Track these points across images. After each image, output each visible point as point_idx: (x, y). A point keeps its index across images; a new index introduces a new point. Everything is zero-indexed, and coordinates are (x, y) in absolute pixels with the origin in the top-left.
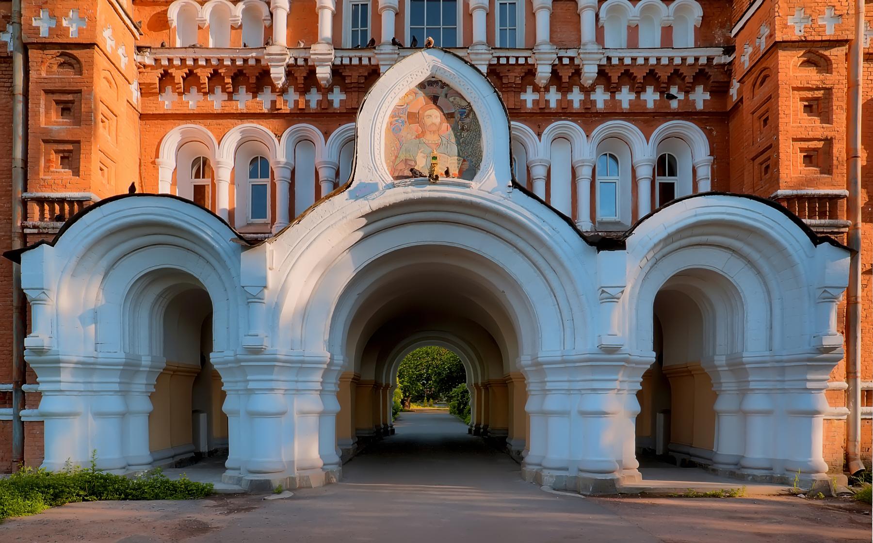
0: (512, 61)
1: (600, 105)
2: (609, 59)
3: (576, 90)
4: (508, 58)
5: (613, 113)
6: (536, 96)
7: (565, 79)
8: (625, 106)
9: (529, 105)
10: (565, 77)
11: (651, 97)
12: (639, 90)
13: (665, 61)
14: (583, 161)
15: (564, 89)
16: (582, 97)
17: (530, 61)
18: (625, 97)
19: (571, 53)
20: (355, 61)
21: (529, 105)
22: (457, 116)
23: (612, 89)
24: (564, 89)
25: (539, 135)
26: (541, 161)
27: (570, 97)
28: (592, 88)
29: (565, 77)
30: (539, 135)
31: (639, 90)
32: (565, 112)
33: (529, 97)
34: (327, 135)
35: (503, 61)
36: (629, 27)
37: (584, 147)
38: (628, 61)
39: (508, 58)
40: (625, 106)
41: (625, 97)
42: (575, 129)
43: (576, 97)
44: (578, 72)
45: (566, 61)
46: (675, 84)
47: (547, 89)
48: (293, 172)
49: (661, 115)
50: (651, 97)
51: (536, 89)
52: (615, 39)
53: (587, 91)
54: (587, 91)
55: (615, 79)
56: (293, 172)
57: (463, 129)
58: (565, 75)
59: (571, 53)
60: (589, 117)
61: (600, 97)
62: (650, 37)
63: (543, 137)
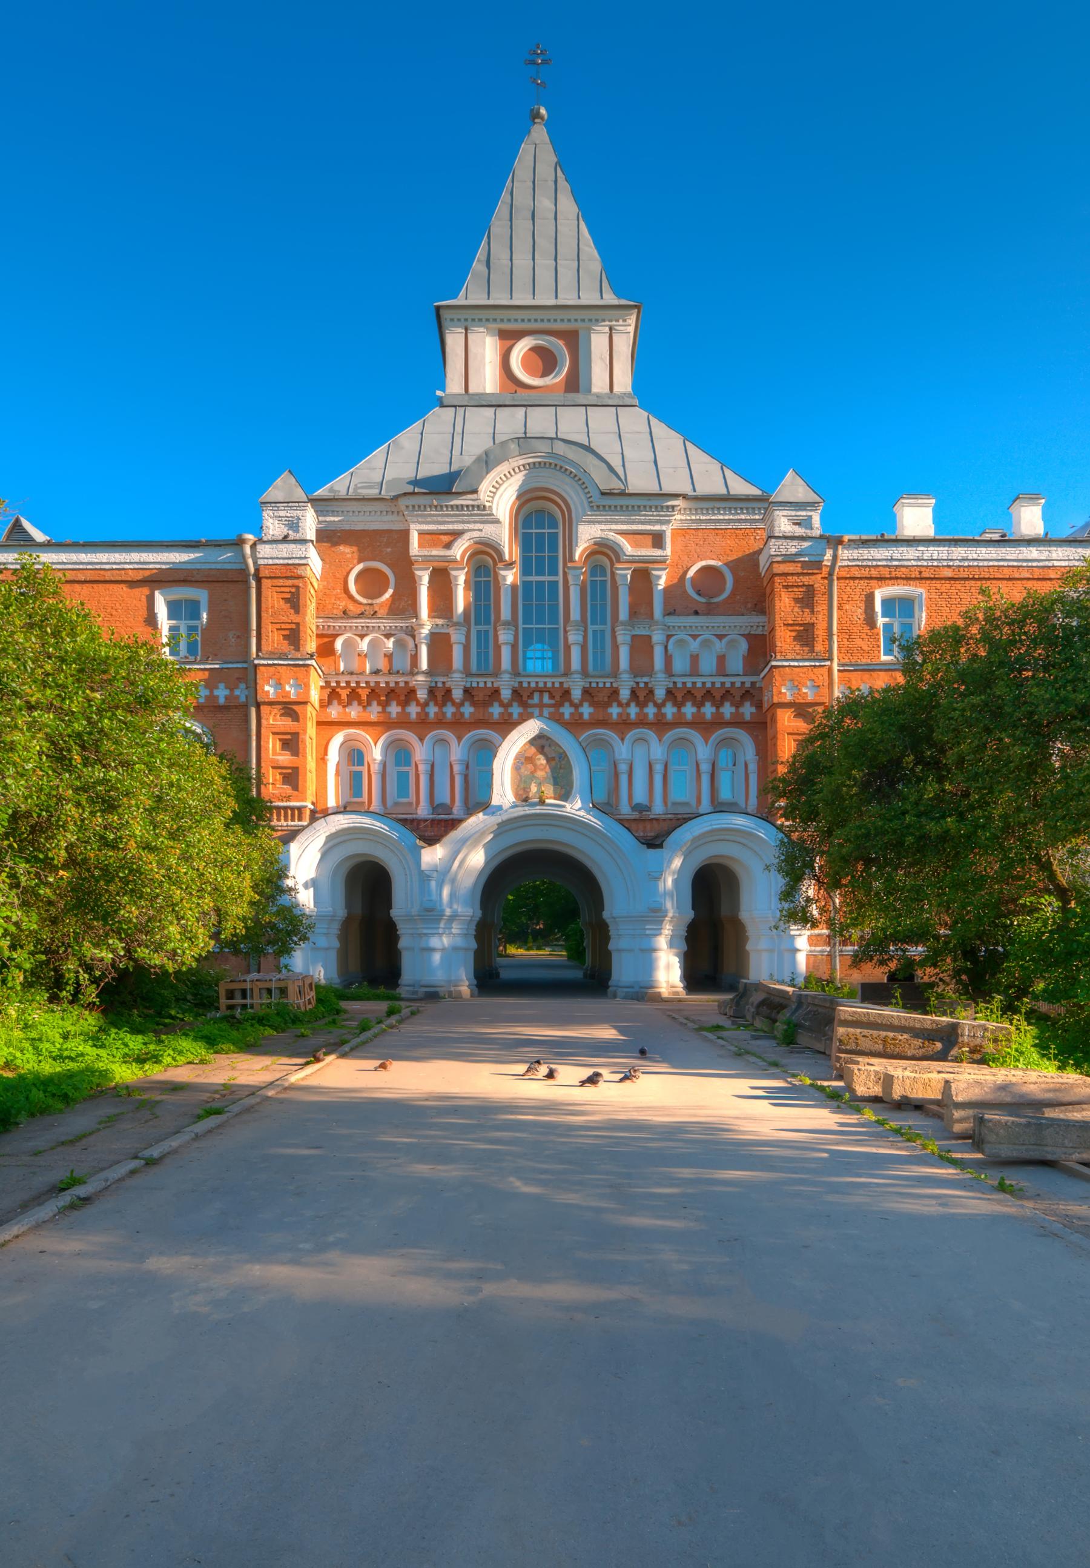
0: (601, 685)
1: (669, 717)
5: (679, 722)
6: (619, 710)
7: (642, 698)
9: (615, 716)
10: (642, 696)
11: (708, 710)
12: (699, 705)
13: (718, 685)
15: (642, 705)
17: (615, 685)
18: (689, 710)
19: (646, 679)
21: (615, 716)
23: (679, 705)
24: (642, 705)
25: (623, 740)
27: (646, 710)
28: (663, 704)
29: (642, 696)
30: (623, 740)
31: (699, 705)
32: (642, 722)
33: (614, 711)
35: (594, 685)
38: (689, 685)
41: (689, 710)
42: (651, 735)
43: (651, 711)
44: (651, 692)
47: (628, 705)
49: (718, 723)
50: (708, 710)
51: (620, 705)
52: (680, 664)
54: (659, 706)
55: (679, 698)
59: (646, 679)
60: (661, 725)
61: (669, 711)
62: (708, 664)
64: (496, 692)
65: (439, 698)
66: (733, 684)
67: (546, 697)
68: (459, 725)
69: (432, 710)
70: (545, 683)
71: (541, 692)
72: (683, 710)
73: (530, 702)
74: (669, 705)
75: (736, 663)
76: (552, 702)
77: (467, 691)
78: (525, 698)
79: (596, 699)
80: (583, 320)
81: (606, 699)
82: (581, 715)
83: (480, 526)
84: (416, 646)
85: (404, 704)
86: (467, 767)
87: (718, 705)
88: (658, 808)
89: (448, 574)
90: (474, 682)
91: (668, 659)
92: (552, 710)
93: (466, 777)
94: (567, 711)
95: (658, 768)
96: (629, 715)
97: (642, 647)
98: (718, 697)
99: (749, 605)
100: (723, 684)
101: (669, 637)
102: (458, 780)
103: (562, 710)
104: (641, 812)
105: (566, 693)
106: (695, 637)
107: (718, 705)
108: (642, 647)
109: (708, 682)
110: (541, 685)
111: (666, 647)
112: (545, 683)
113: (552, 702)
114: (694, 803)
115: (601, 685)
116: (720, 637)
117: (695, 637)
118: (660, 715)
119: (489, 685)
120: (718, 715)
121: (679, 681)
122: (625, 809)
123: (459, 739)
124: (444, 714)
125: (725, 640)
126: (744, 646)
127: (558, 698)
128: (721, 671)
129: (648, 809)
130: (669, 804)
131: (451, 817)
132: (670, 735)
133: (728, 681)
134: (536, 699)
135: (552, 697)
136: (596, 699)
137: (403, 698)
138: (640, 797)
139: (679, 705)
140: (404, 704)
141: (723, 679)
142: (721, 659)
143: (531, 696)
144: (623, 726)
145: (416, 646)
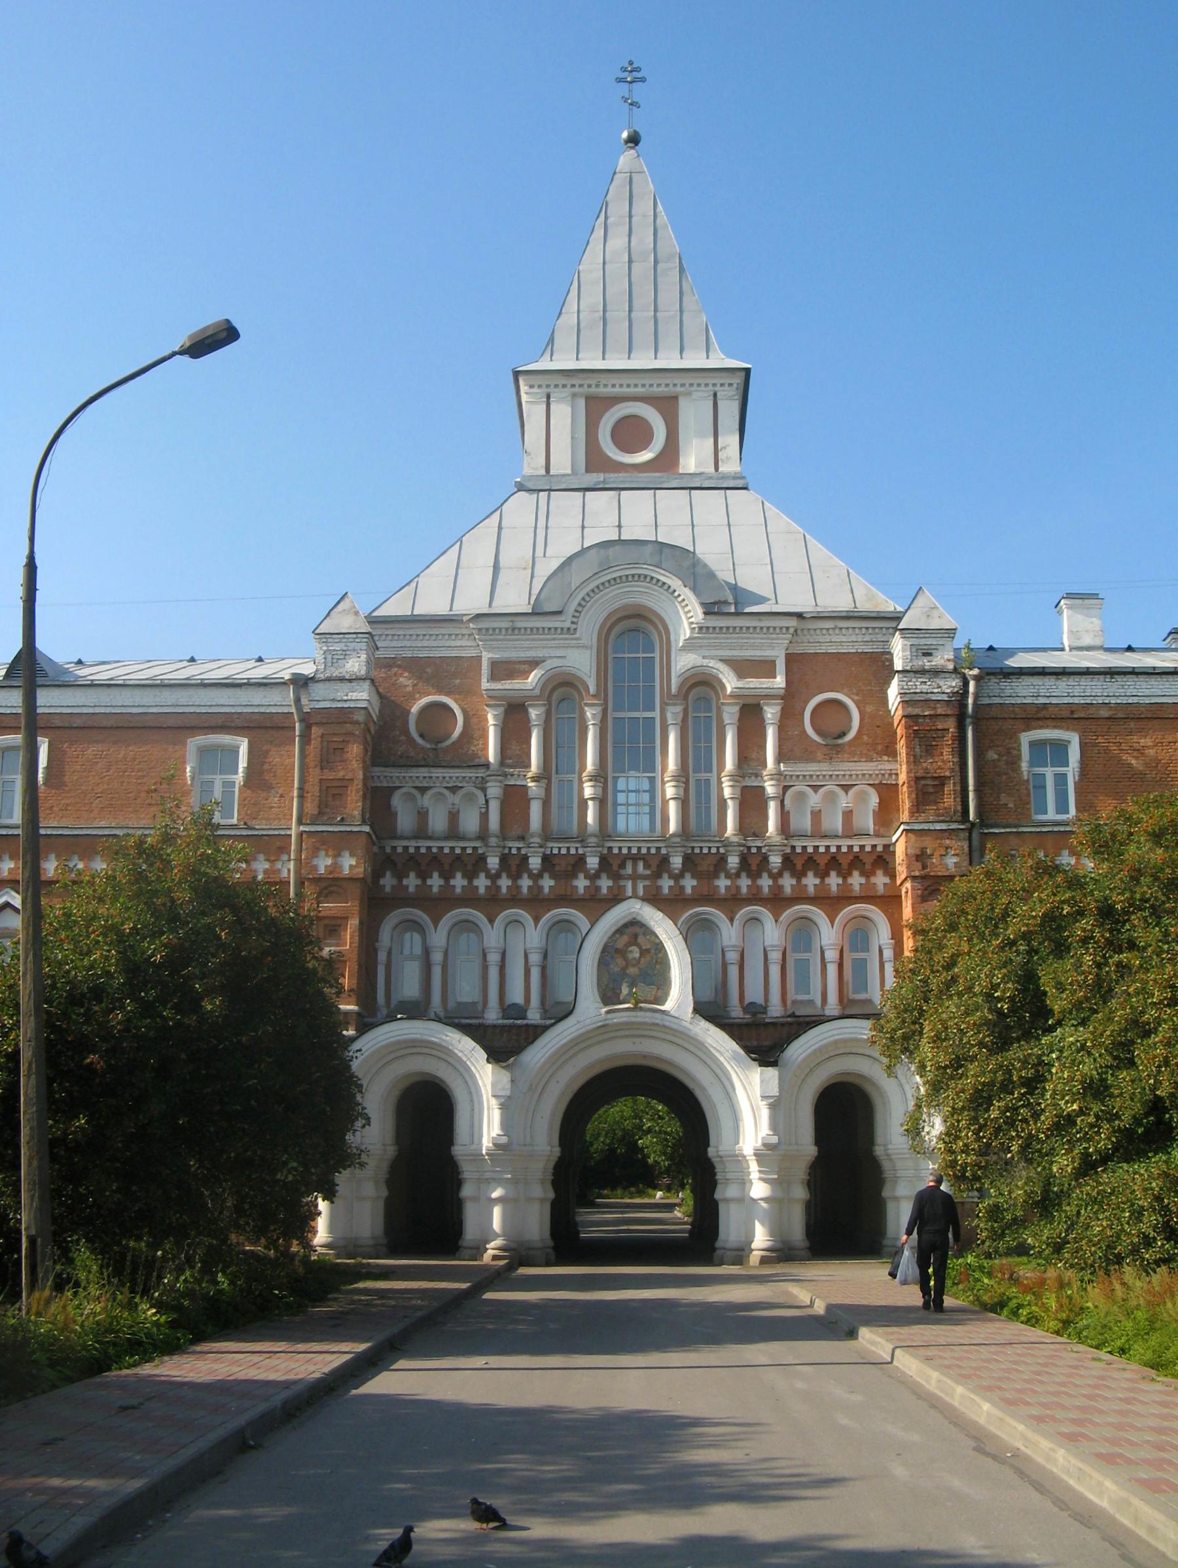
0: (705, 851)
1: (788, 890)
2: (793, 847)
3: (765, 875)
4: (701, 848)
6: (728, 882)
7: (754, 867)
8: (811, 890)
10: (754, 863)
11: (834, 881)
14: (772, 946)
15: (755, 875)
16: (770, 882)
17: (722, 850)
20: (564, 851)
22: (653, 951)
23: (799, 875)
24: (755, 875)
25: (732, 920)
26: (734, 946)
27: (760, 882)
30: (732, 920)
31: (823, 875)
33: (722, 883)
34: (537, 920)
35: (697, 851)
36: (813, 813)
37: (772, 932)
39: (701, 848)
40: (811, 890)
43: (765, 882)
45: (754, 850)
46: (856, 869)
47: (738, 875)
48: (504, 954)
50: (834, 881)
51: (728, 876)
53: (775, 877)
54: (775, 877)
55: (799, 867)
56: (504, 954)
57: (656, 962)
58: (754, 863)
60: (777, 902)
61: (788, 882)
63: (736, 923)
64: (581, 860)
65: (514, 868)
66: (862, 847)
67: (641, 864)
68: (537, 903)
69: (505, 883)
70: (639, 848)
71: (635, 859)
72: (804, 881)
73: (623, 872)
74: (787, 875)
75: (867, 821)
76: (648, 872)
77: (546, 859)
78: (615, 867)
79: (699, 869)
80: (683, 385)
81: (712, 868)
82: (682, 888)
83: (558, 653)
84: (487, 801)
85: (470, 876)
86: (545, 956)
87: (845, 875)
88: (775, 1010)
89: (527, 713)
90: (555, 847)
91: (784, 816)
92: (647, 883)
93: (544, 969)
94: (666, 884)
95: (775, 956)
96: (738, 888)
97: (751, 802)
98: (845, 866)
99: (880, 748)
100: (850, 847)
101: (786, 788)
102: (535, 974)
103: (660, 882)
104: (754, 1014)
105: (665, 860)
106: (815, 788)
107: (845, 875)
108: (751, 802)
109: (833, 844)
110: (634, 851)
111: (782, 802)
112: (639, 848)
113: (648, 872)
114: (819, 1002)
115: (705, 851)
116: (846, 788)
117: (815, 788)
118: (777, 889)
119: (573, 851)
120: (845, 886)
121: (799, 844)
122: (736, 1012)
123: (537, 920)
124: (519, 888)
125: (851, 792)
126: (874, 800)
127: (654, 868)
128: (850, 832)
129: (764, 1009)
130: (789, 1002)
131: (525, 1022)
132: (789, 913)
133: (856, 843)
134: (629, 870)
135: (647, 866)
136: (699, 869)
137: (470, 868)
138: (754, 994)
139: (799, 875)
140: (470, 876)
141: (850, 842)
142: (848, 814)
143: (622, 866)
144: (732, 903)
145: (487, 801)
